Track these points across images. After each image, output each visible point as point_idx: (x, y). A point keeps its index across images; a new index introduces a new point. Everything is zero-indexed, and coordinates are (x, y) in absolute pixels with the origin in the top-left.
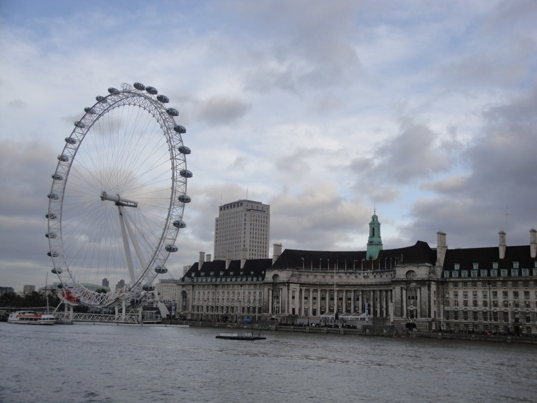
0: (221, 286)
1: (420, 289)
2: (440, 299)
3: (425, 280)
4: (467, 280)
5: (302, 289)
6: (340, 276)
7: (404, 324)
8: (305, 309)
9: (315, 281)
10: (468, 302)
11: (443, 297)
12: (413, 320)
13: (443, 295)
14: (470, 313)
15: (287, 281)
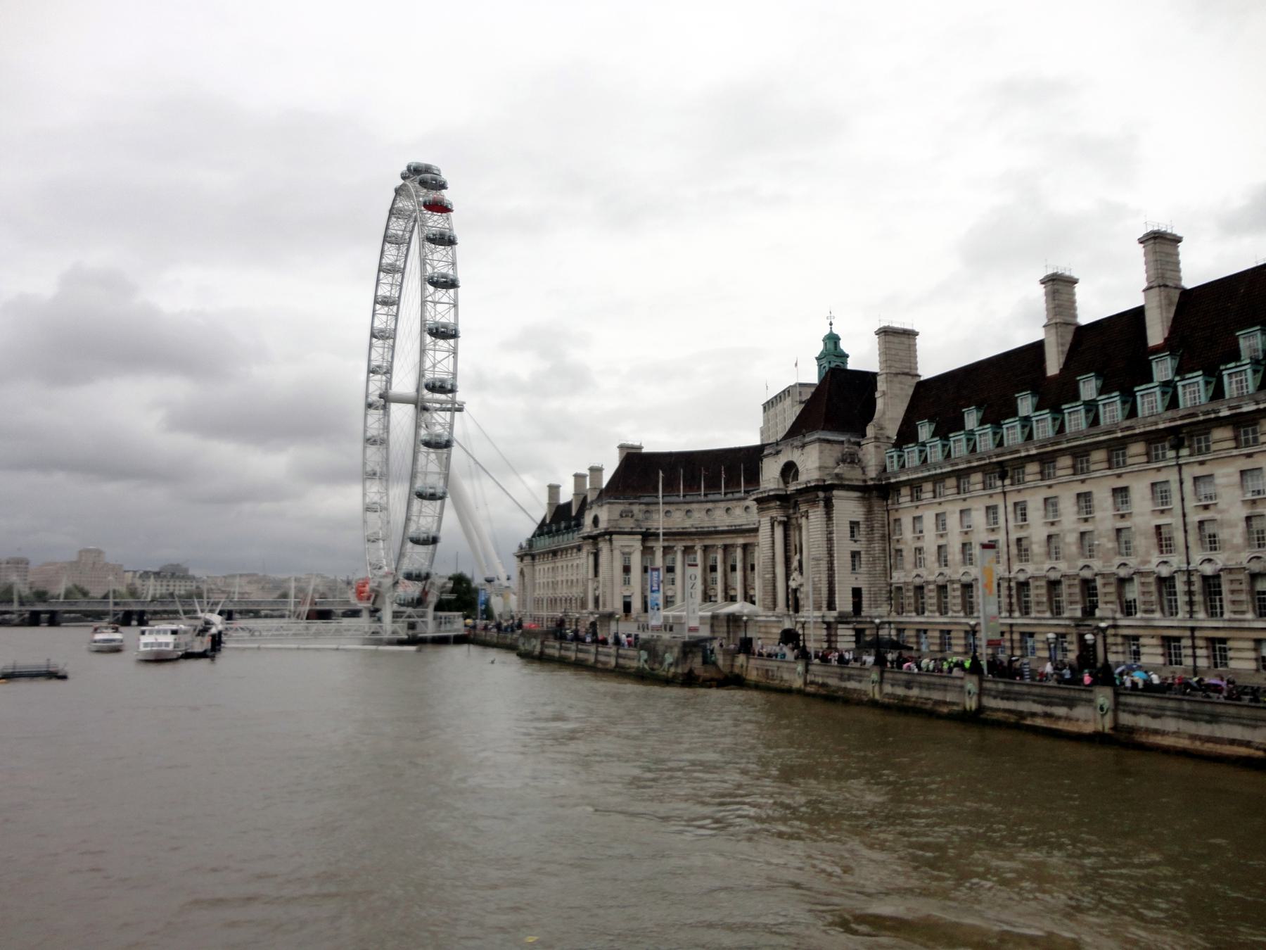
0: (560, 553)
1: (807, 518)
2: (877, 546)
3: (811, 487)
4: (939, 471)
5: (652, 548)
6: (747, 508)
7: (776, 631)
8: (671, 597)
9: (688, 524)
10: (950, 550)
11: (887, 538)
12: (793, 619)
13: (887, 532)
14: (954, 590)
15: (608, 529)
